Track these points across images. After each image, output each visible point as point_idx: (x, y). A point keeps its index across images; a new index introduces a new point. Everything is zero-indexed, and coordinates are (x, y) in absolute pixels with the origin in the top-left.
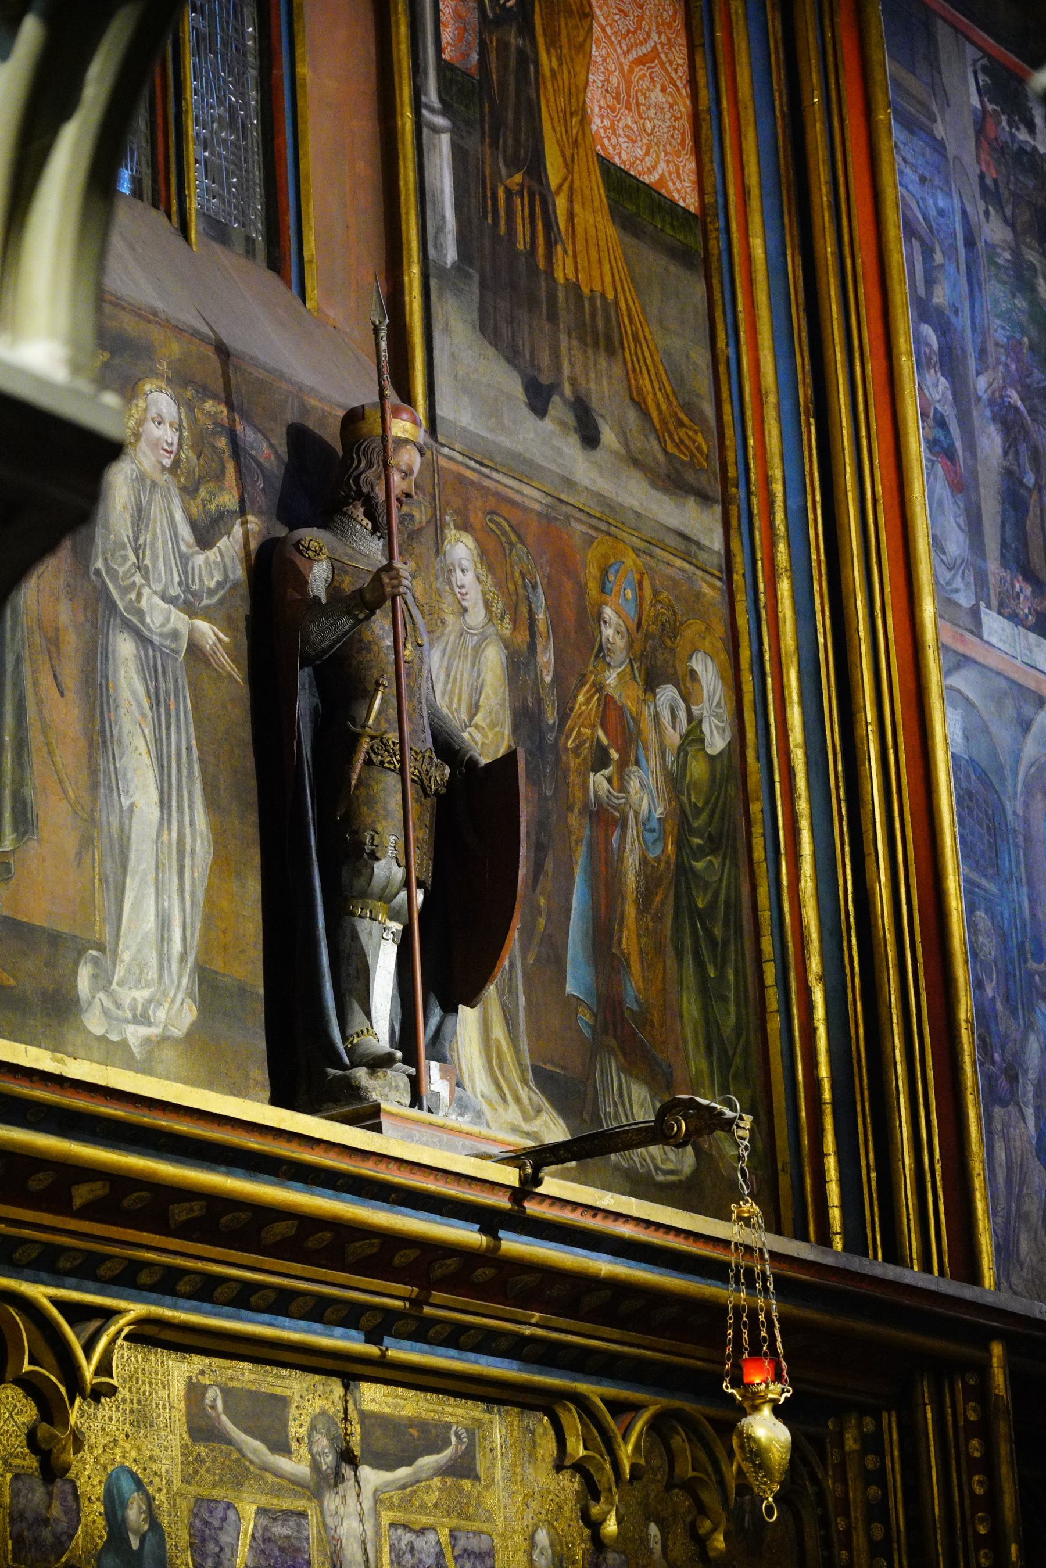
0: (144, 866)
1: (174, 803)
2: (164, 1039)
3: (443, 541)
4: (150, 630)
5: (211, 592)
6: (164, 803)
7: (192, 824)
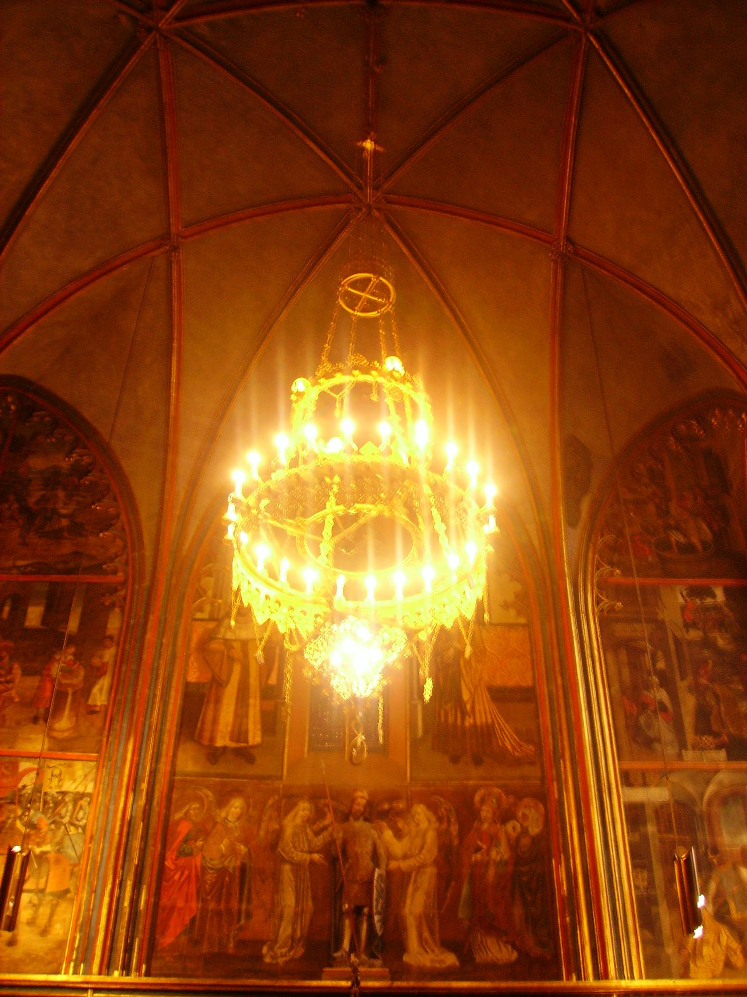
6: (297, 901)
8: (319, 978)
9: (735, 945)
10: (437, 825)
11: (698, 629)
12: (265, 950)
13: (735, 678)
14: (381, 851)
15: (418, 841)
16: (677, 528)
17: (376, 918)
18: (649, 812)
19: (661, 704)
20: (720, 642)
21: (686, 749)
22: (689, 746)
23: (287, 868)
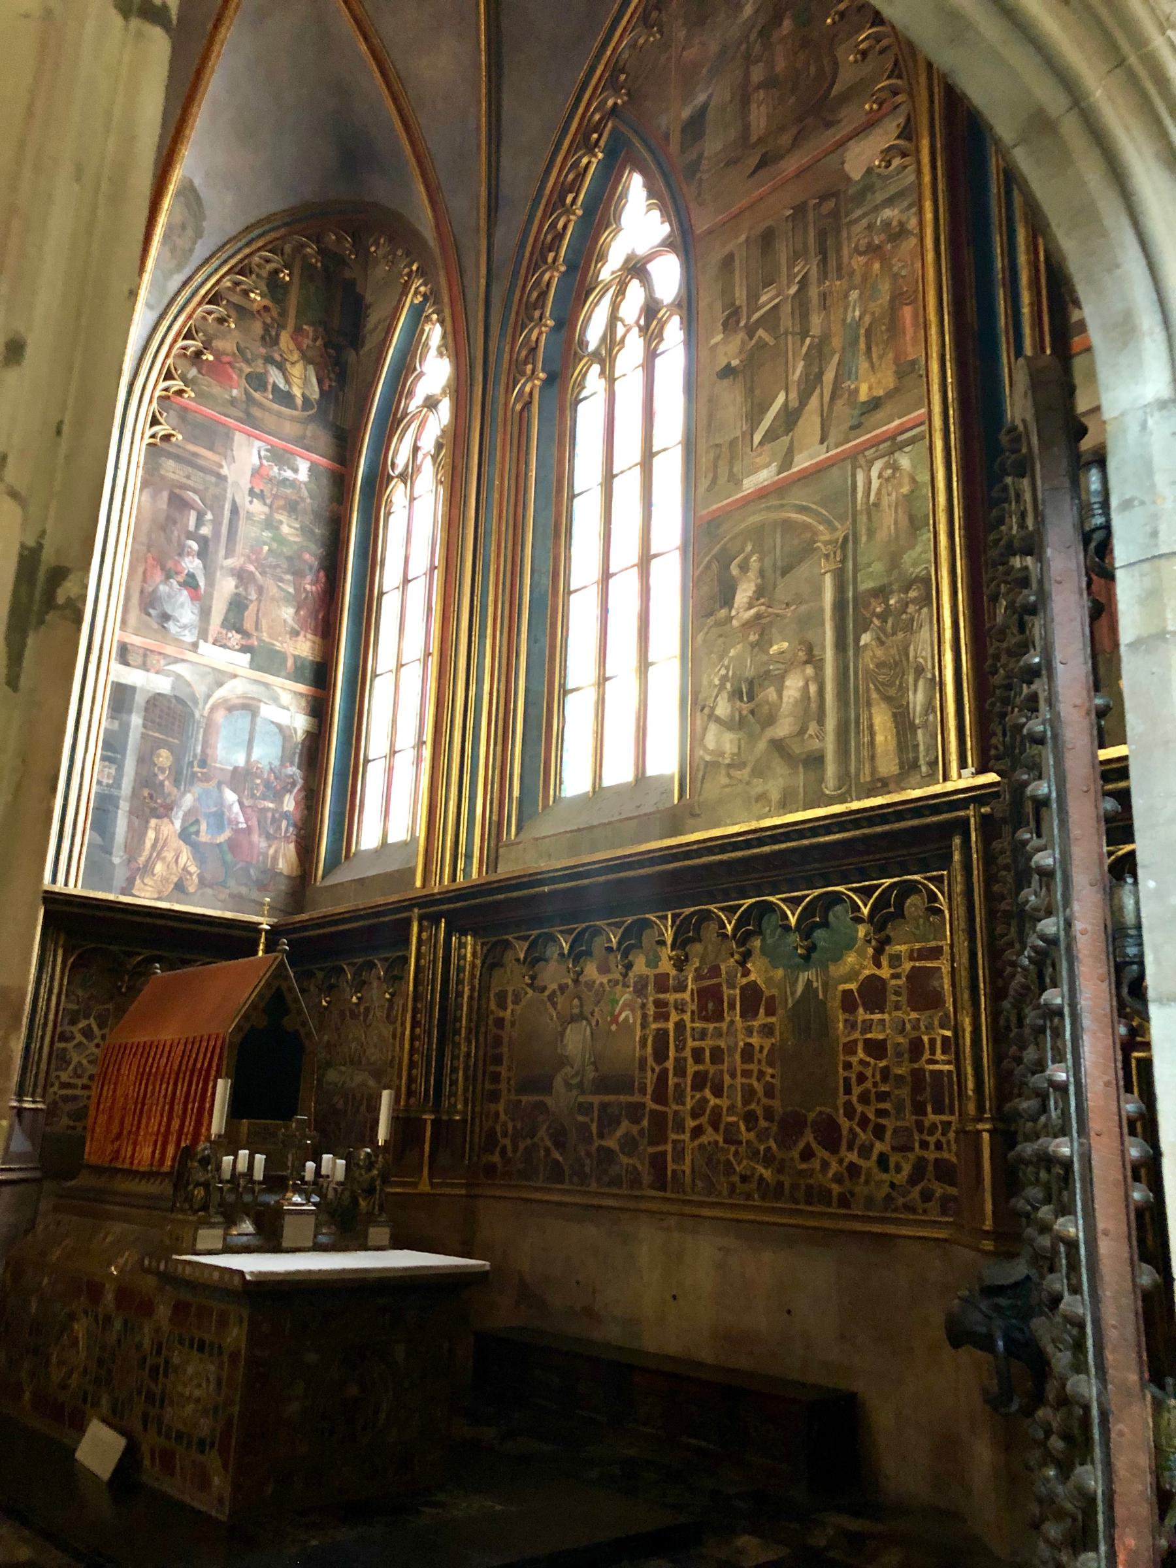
9: (193, 869)
11: (265, 504)
13: (289, 577)
16: (281, 367)
18: (140, 700)
19: (191, 576)
20: (285, 529)
21: (206, 641)
22: (211, 639)
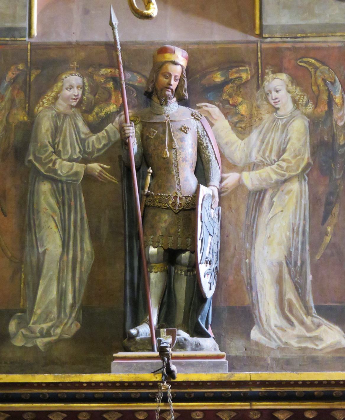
0: (51, 273)
1: (71, 243)
2: (60, 340)
3: (263, 81)
4: (60, 176)
5: (99, 150)
7: (82, 249)
8: (107, 370)
10: (310, 108)
12: (12, 326)
14: (213, 155)
15: (275, 138)
17: (203, 269)
23: (45, 187)
